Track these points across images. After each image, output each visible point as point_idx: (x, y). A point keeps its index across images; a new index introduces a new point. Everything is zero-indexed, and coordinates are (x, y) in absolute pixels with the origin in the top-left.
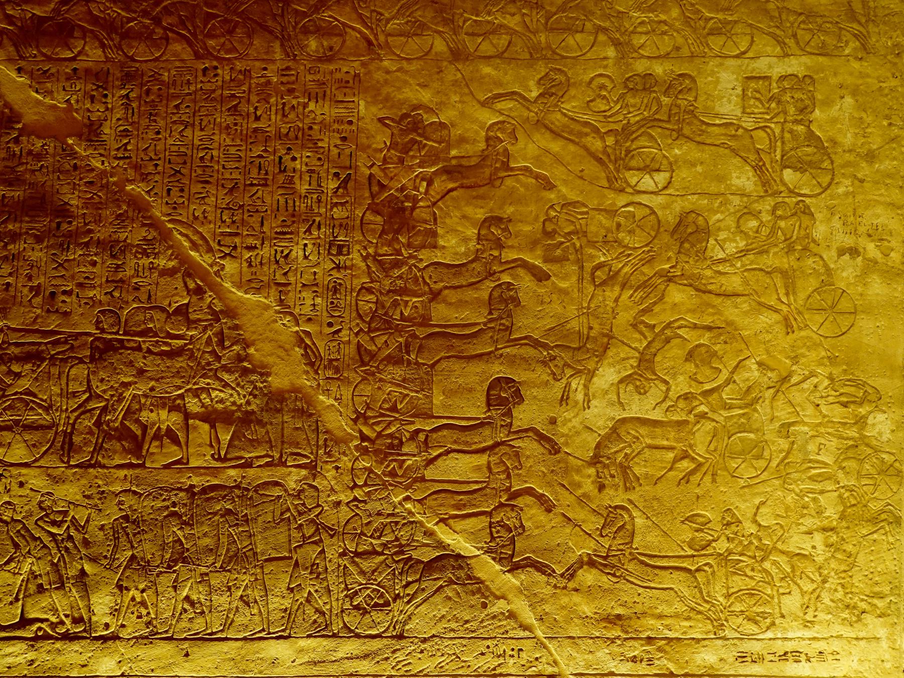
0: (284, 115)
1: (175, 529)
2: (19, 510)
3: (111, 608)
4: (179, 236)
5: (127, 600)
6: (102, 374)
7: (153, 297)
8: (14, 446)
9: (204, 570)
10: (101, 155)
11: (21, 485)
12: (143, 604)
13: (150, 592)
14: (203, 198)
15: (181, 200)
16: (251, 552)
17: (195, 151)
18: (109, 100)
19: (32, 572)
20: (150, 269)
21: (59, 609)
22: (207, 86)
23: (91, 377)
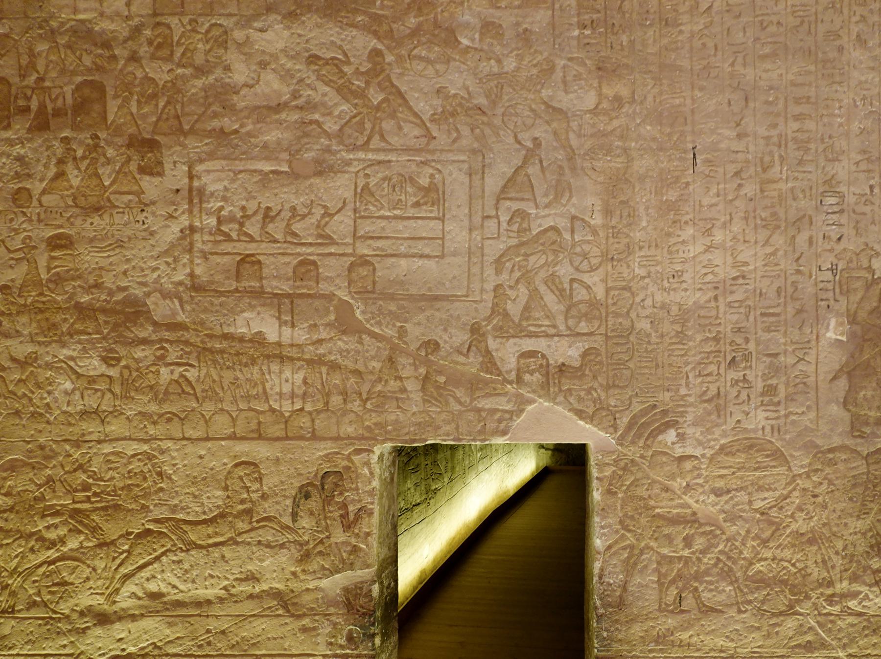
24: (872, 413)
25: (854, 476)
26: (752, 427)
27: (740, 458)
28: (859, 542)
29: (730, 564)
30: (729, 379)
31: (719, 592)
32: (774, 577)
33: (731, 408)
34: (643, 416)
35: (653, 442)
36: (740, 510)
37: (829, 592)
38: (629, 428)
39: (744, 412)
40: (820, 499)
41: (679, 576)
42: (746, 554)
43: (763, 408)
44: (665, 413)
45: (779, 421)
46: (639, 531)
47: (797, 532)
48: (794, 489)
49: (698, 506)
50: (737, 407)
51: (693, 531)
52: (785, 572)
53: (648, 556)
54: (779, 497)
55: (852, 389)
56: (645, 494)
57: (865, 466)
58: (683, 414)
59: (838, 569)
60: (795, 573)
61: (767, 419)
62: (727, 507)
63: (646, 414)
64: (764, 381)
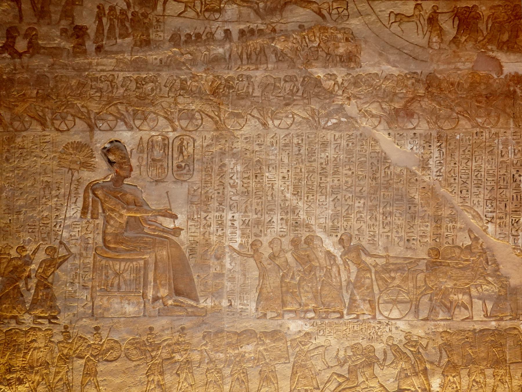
0: (515, 155)
1: (468, 349)
2: (395, 340)
3: (440, 384)
4: (466, 213)
5: (447, 381)
6: (432, 278)
7: (455, 242)
8: (393, 311)
9: (482, 367)
10: (429, 175)
11: (397, 328)
12: (454, 382)
13: (457, 377)
14: (477, 195)
15: (467, 196)
16: (503, 360)
17: (473, 173)
18: (432, 148)
19: (402, 368)
20: (453, 228)
21: (416, 384)
22: (478, 141)
23: (427, 279)
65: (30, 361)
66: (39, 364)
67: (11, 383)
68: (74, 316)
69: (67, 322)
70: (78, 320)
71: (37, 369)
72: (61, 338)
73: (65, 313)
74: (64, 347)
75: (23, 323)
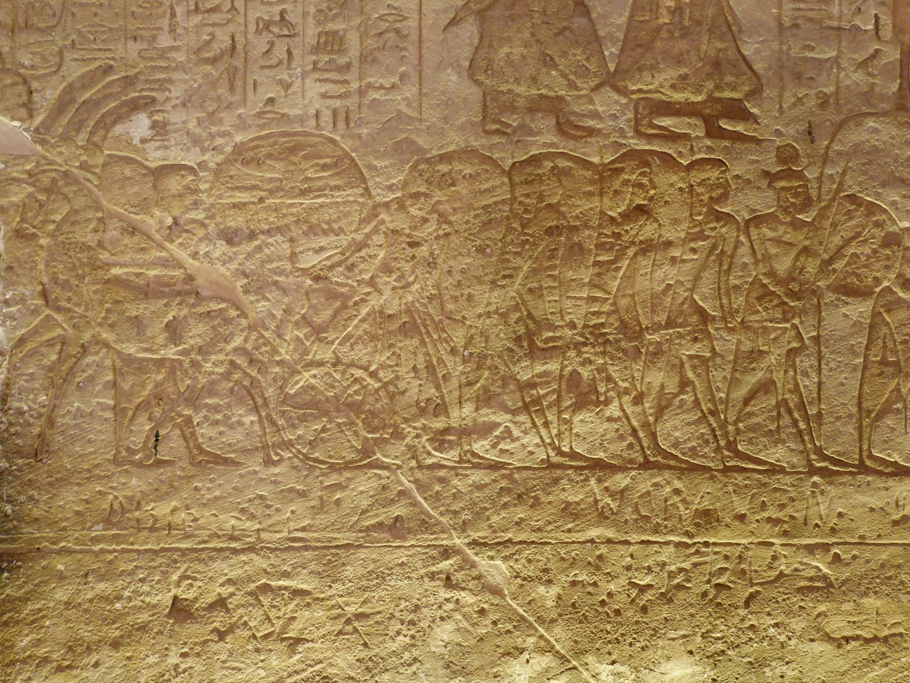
24: (522, 90)
25: (485, 207)
26: (297, 111)
27: (273, 172)
28: (496, 330)
29: (254, 373)
30: (252, 18)
31: (232, 427)
32: (336, 397)
33: (256, 74)
34: (85, 87)
35: (105, 138)
36: (274, 271)
37: (439, 424)
38: (61, 107)
39: (281, 82)
40: (423, 251)
41: (158, 397)
42: (285, 353)
43: (317, 75)
44: (129, 82)
45: (348, 102)
46: (80, 310)
47: (381, 313)
48: (376, 231)
49: (196, 263)
50: (267, 72)
51: (185, 311)
52: (356, 387)
53: (97, 358)
54: (350, 246)
55: (484, 42)
56: (91, 239)
57: (507, 188)
58: (163, 85)
59: (455, 382)
60: (377, 391)
61: (324, 96)
62: (250, 266)
63: (93, 83)
64: (319, 23)
65: (623, 302)
66: (662, 318)
67: (537, 401)
68: (824, 105)
69: (791, 131)
70: (841, 125)
71: (656, 337)
72: (763, 201)
73: (782, 90)
74: (778, 241)
75: (591, 132)
